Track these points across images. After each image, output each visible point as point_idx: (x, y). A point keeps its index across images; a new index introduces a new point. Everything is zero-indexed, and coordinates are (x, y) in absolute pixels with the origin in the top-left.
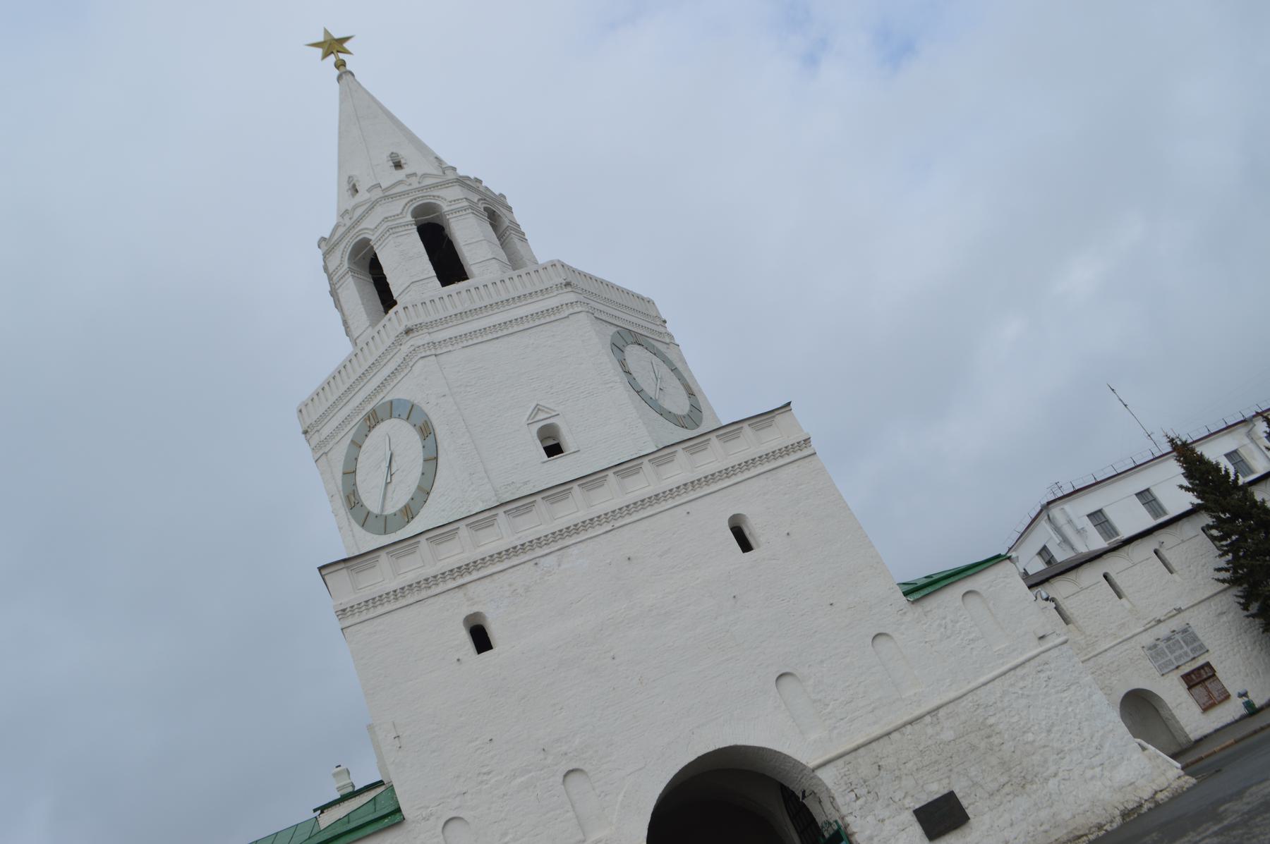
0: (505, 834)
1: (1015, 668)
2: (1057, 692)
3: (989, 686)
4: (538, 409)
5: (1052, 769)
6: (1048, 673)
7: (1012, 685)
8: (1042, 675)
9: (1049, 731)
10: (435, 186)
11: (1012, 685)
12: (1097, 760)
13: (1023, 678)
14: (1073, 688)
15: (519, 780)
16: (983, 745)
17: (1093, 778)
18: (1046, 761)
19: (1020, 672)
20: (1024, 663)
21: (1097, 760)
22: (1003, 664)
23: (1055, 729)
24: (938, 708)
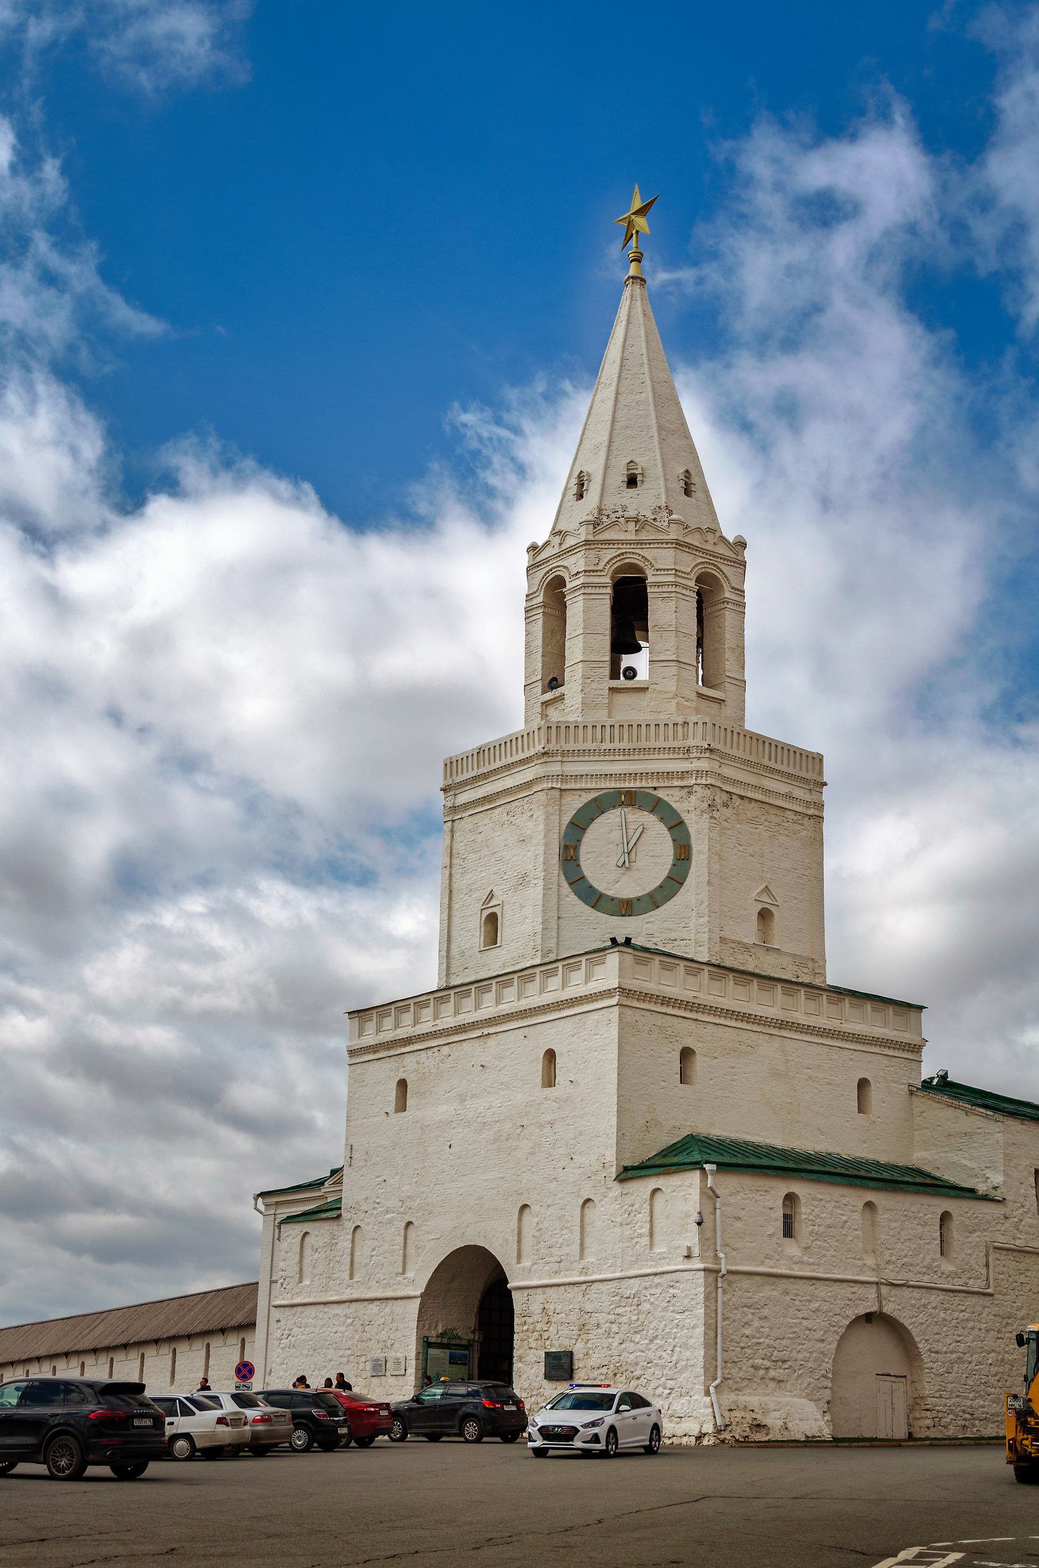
0: (374, 1249)
1: (656, 1274)
2: (673, 1312)
3: (632, 1280)
4: (491, 895)
5: (637, 1373)
6: (676, 1291)
7: (646, 1288)
8: (671, 1291)
9: (651, 1341)
10: (571, 550)
11: (646, 1288)
12: (670, 1383)
13: (657, 1286)
14: (686, 1313)
15: (389, 1216)
16: (605, 1327)
17: (659, 1396)
18: (637, 1364)
19: (657, 1280)
20: (663, 1273)
21: (670, 1383)
22: (655, 1266)
23: (656, 1341)
24: (593, 1282)
